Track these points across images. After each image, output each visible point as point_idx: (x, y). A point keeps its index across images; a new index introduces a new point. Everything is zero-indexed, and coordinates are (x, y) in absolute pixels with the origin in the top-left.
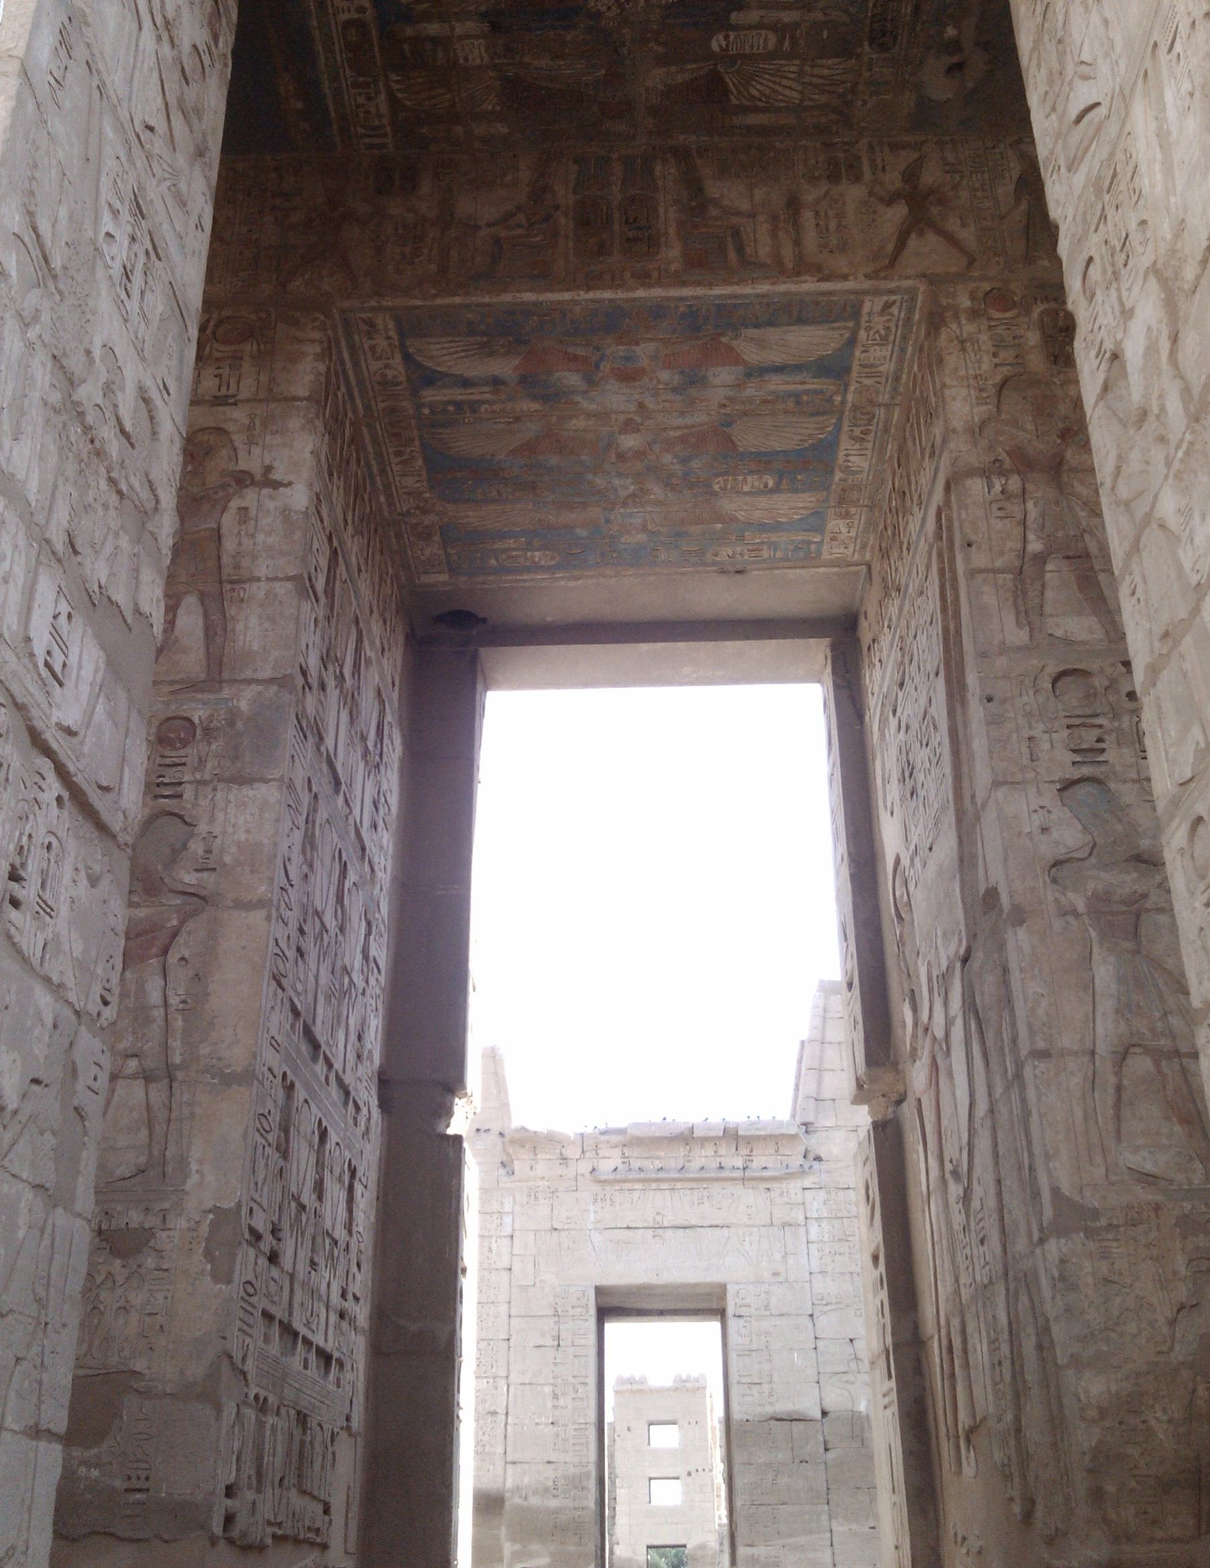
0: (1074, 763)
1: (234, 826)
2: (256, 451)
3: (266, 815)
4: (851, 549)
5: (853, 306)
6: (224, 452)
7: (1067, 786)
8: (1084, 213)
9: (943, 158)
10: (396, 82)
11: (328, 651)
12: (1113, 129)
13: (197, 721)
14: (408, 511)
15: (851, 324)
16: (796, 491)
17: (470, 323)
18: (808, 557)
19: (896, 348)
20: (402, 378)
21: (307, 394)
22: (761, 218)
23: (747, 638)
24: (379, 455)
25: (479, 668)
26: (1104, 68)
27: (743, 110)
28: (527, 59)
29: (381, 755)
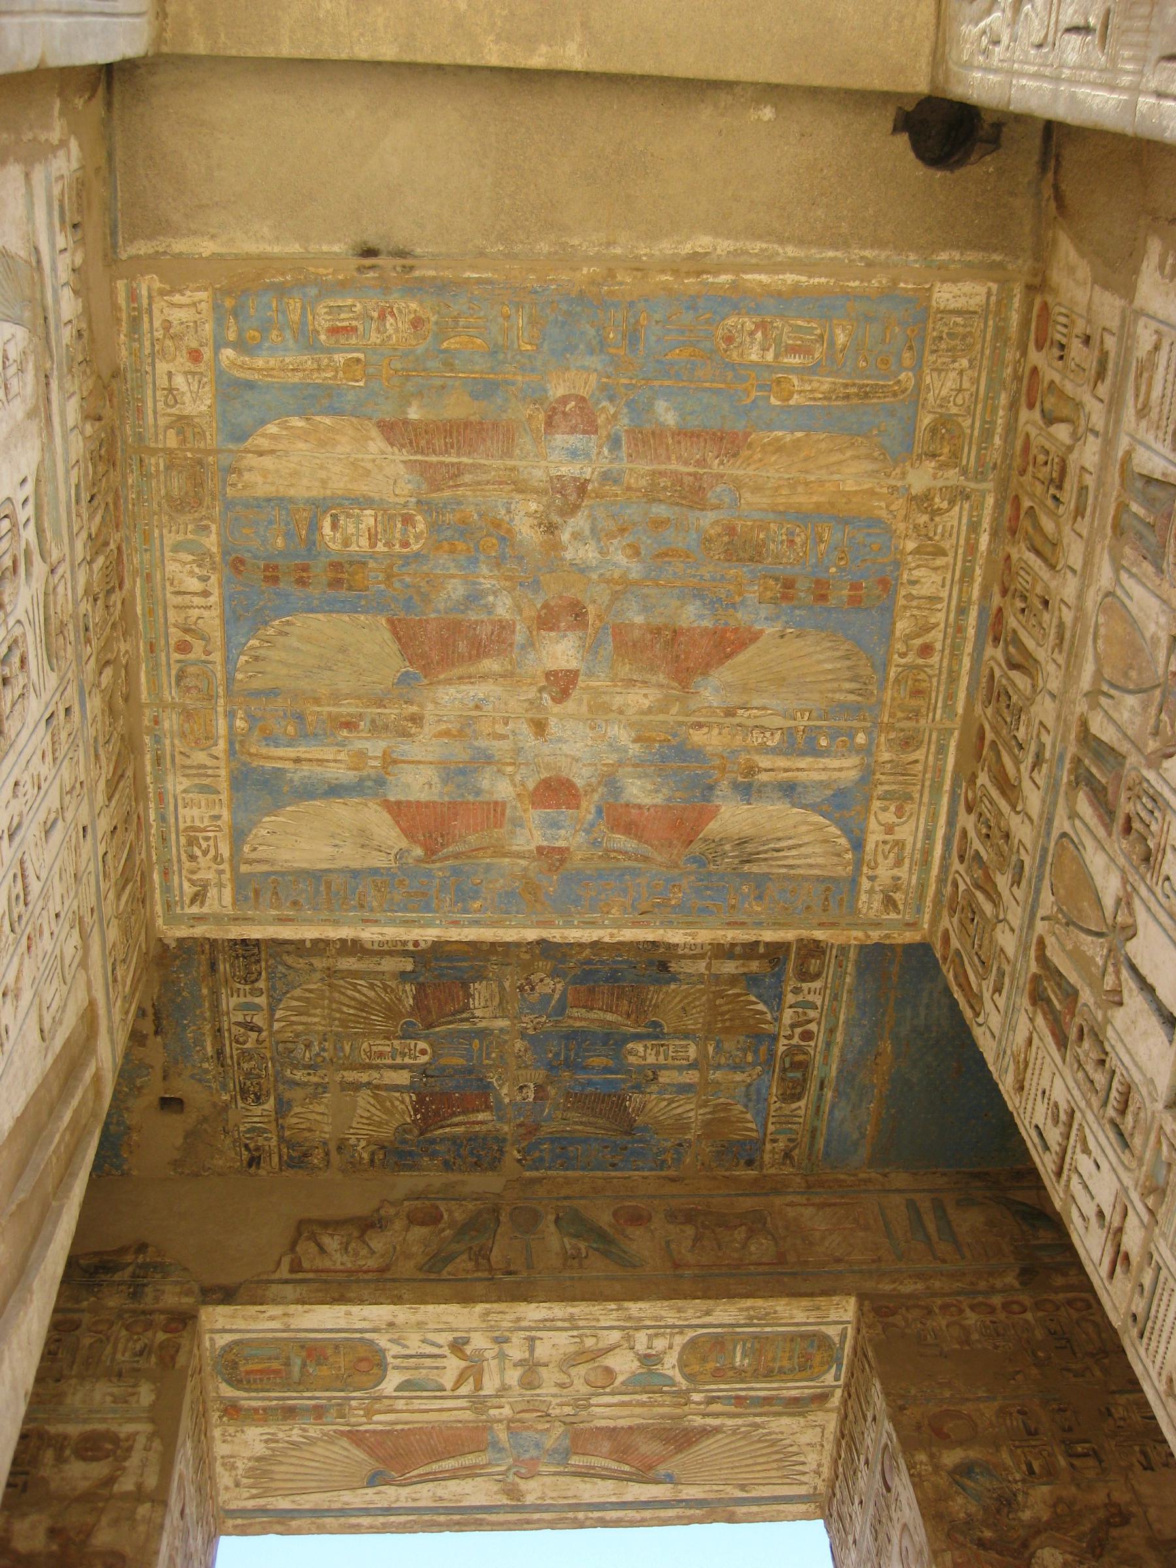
4: (157, 324)
14: (952, 503)
15: (244, 868)
16: (280, 502)
17: (759, 898)
18: (243, 291)
19: (172, 821)
20: (876, 804)
24: (955, 653)
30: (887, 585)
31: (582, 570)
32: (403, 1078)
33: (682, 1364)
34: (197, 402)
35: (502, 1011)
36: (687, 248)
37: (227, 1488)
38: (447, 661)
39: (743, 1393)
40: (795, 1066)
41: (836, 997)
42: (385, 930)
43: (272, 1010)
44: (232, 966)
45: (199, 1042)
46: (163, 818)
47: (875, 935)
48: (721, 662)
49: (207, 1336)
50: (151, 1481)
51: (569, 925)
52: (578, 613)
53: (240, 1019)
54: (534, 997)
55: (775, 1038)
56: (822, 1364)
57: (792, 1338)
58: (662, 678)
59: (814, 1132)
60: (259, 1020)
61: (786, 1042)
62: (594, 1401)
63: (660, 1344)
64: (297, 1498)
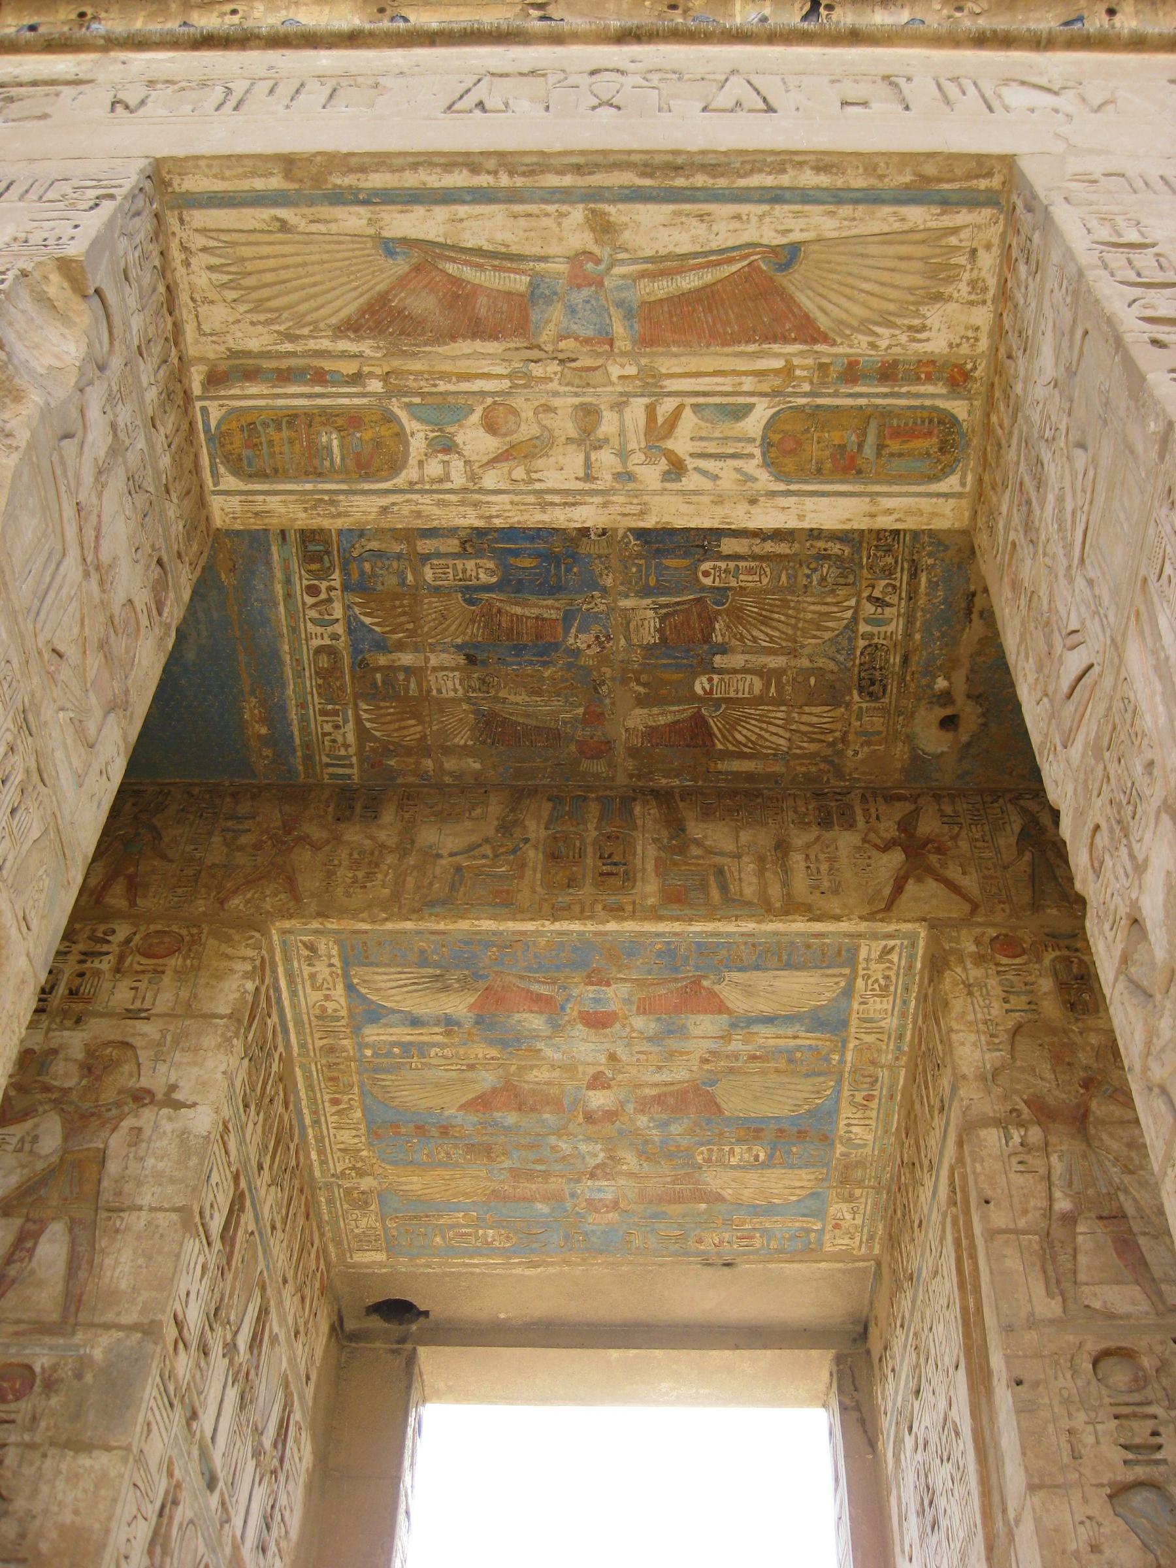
0: (1125, 1462)
1: (60, 1504)
2: (162, 1068)
3: (103, 1492)
4: (858, 1239)
5: (848, 950)
6: (126, 1068)
7: (1119, 1492)
8: (1086, 781)
9: (940, 810)
10: (365, 711)
11: (217, 1310)
12: (1108, 683)
13: (38, 1369)
14: (343, 1173)
15: (847, 971)
17: (422, 952)
20: (344, 1013)
21: (228, 1012)
22: (746, 859)
23: (737, 1347)
24: (313, 1101)
25: (416, 1371)
26: (1093, 627)
27: (726, 755)
28: (501, 695)
29: (282, 1461)
30: (374, 1134)
31: (589, 1139)
33: (401, 436)
35: (627, 616)
36: (539, 1270)
37: (988, 247)
38: (684, 1093)
39: (318, 389)
41: (294, 630)
42: (735, 929)
43: (855, 619)
44: (887, 661)
45: (932, 586)
48: (484, 1094)
49: (968, 489)
53: (887, 610)
54: (596, 629)
55: (346, 587)
56: (229, 433)
57: (275, 473)
58: (526, 1086)
60: (869, 609)
61: (333, 583)
62: (505, 384)
63: (434, 468)
64: (897, 226)
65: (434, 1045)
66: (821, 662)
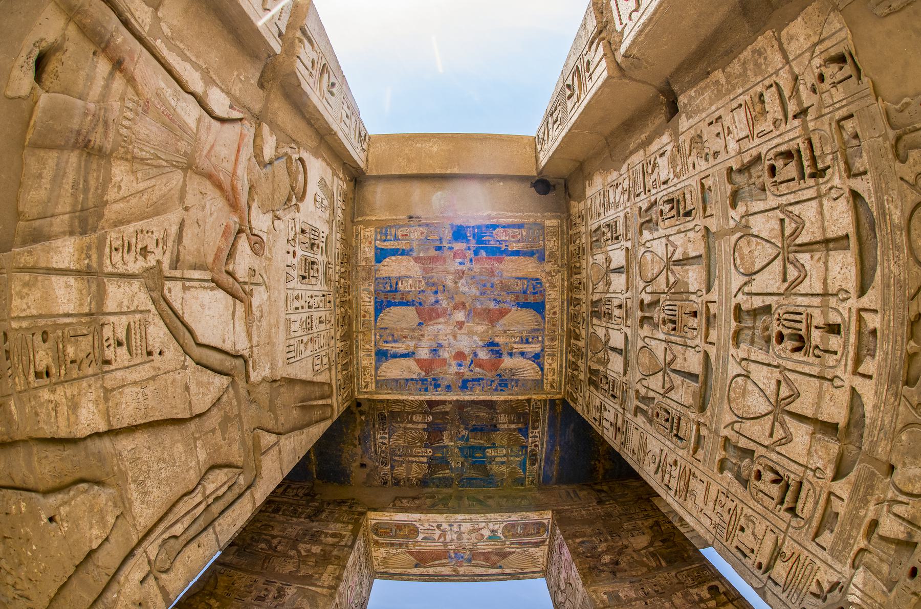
18: (383, 229)
24: (562, 313)
32: (425, 460)
33: (503, 533)
34: (371, 254)
40: (533, 455)
41: (543, 434)
46: (357, 364)
47: (549, 396)
50: (349, 544)
51: (465, 395)
52: (463, 305)
54: (460, 436)
55: (527, 447)
57: (534, 524)
59: (539, 475)
60: (386, 441)
63: (496, 527)
65: (517, 343)
66: (397, 425)
